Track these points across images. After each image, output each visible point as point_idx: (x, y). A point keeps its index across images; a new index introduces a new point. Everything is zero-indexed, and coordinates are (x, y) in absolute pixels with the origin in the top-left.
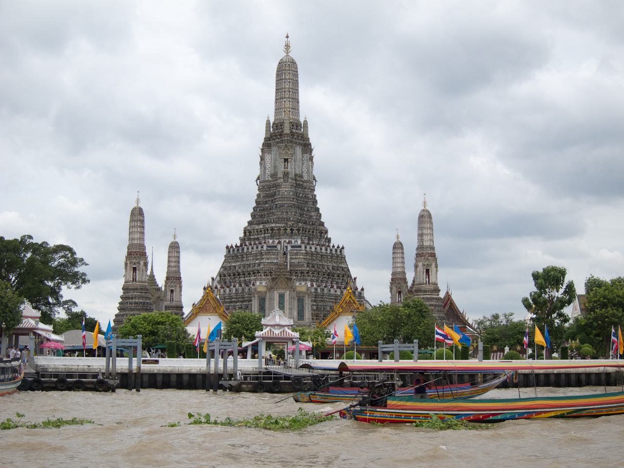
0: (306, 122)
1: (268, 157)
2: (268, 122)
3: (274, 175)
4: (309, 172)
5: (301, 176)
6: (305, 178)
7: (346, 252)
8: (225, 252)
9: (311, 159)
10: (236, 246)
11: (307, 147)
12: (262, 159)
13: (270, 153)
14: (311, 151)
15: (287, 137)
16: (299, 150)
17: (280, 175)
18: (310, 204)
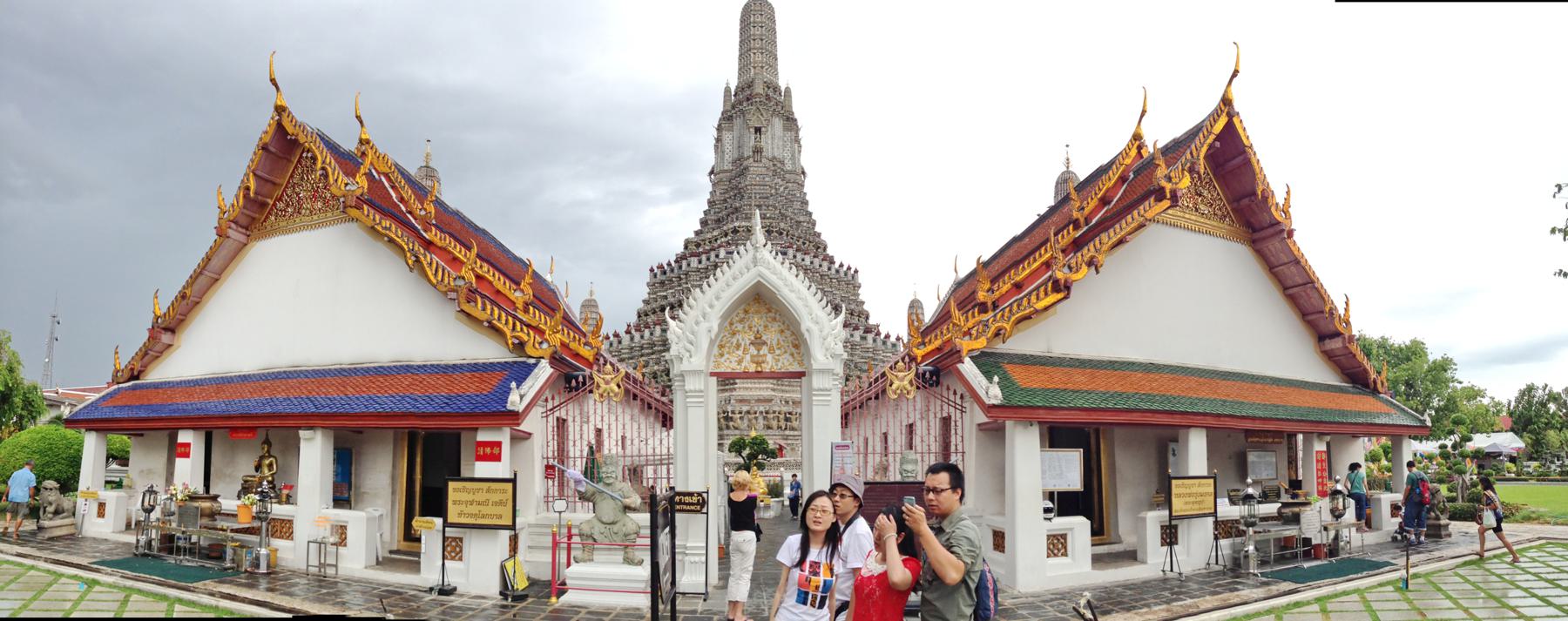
0: (788, 90)
1: (727, 136)
2: (727, 90)
3: (739, 160)
4: (795, 157)
5: (782, 163)
6: (788, 167)
7: (861, 278)
8: (647, 277)
9: (797, 141)
10: (669, 264)
11: (790, 122)
12: (718, 140)
13: (731, 129)
14: (797, 130)
15: (756, 104)
16: (778, 123)
17: (748, 152)
18: (797, 205)
